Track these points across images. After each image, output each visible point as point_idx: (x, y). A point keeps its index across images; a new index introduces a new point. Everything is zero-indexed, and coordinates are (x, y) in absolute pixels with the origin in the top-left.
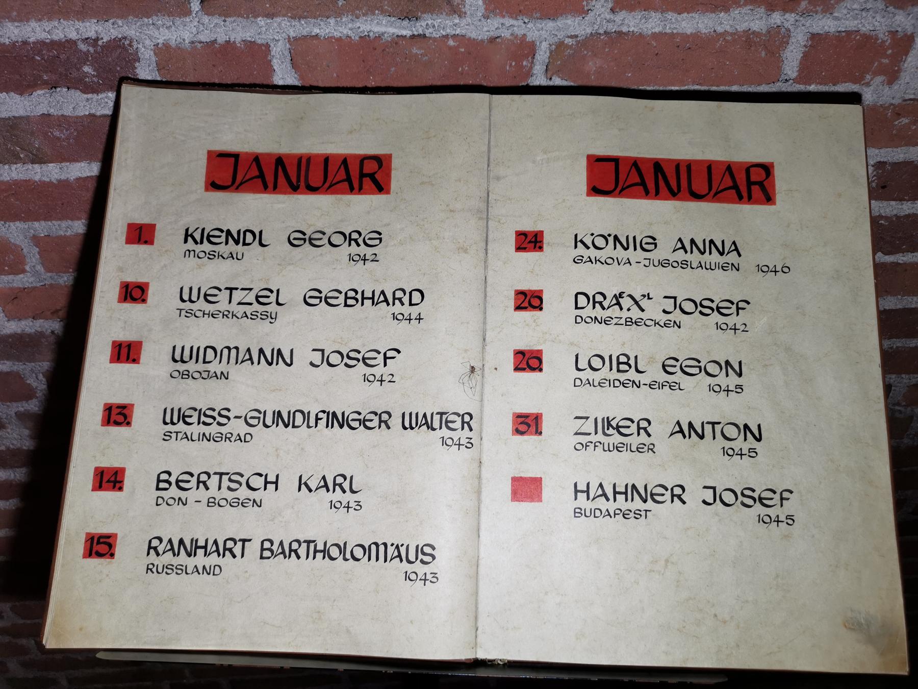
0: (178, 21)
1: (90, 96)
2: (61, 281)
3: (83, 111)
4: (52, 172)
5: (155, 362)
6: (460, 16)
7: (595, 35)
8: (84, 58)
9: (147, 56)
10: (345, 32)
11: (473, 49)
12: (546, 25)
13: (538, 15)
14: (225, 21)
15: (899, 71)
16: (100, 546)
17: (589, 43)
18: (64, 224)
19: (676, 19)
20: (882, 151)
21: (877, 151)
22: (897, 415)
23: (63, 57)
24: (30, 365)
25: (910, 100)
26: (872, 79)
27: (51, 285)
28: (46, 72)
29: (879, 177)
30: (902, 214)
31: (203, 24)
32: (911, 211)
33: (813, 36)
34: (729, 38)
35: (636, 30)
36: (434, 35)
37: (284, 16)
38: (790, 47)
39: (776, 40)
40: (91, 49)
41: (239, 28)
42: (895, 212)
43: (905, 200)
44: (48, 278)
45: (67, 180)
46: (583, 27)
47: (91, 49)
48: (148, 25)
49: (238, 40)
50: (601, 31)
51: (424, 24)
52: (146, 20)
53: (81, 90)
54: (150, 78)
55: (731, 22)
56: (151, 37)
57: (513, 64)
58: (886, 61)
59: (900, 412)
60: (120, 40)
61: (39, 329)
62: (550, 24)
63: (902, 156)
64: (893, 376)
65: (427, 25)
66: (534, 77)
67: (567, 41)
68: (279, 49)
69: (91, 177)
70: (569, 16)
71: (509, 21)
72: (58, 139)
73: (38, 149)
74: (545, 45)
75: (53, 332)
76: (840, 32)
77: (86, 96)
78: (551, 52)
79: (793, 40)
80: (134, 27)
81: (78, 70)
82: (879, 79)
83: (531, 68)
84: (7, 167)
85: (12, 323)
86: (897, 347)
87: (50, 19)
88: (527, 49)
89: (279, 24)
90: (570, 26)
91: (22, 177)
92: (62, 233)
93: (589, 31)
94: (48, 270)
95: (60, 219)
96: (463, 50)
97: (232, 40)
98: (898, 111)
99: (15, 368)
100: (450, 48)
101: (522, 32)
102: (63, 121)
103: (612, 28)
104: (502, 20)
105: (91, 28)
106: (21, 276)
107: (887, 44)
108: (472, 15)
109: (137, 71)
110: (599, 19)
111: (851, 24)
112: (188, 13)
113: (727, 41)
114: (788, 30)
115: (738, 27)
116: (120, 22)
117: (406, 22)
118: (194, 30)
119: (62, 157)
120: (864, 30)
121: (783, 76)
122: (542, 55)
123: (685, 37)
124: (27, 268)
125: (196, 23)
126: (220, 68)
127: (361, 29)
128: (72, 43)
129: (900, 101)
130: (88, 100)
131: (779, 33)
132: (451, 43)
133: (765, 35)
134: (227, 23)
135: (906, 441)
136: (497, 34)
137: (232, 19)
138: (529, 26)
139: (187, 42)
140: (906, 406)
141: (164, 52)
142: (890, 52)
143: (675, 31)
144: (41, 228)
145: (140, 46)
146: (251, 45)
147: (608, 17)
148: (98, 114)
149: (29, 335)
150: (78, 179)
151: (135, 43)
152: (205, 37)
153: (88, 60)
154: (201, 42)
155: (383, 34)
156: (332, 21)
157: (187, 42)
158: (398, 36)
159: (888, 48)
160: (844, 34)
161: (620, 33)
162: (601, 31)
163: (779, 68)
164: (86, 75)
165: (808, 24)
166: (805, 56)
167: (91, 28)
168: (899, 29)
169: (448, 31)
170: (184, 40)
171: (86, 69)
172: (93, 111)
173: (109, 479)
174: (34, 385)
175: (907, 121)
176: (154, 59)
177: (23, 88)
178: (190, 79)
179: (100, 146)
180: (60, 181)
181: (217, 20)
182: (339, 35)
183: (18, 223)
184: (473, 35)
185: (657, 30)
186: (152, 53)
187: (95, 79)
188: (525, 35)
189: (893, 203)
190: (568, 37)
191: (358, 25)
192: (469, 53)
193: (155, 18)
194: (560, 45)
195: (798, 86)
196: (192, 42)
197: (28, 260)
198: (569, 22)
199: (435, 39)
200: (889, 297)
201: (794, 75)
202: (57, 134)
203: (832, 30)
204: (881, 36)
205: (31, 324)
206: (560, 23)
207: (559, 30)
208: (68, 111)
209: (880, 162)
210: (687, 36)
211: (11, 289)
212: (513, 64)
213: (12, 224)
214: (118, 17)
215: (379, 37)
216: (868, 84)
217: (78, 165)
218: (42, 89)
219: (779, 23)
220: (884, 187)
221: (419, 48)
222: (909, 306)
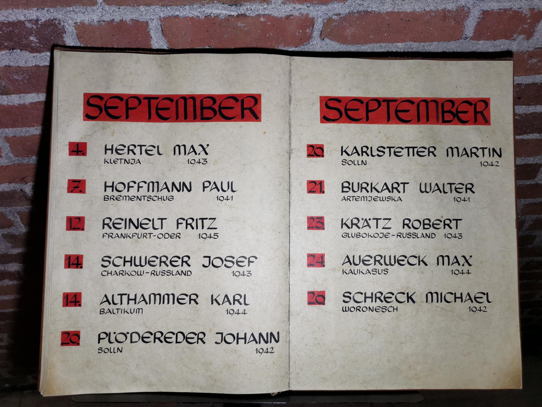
0: (89, 9)
1: (35, 54)
2: (25, 162)
3: (31, 64)
4: (15, 100)
5: (93, 226)
6: (268, 4)
7: (351, 14)
8: (30, 32)
9: (70, 30)
10: (196, 14)
11: (277, 24)
12: (321, 8)
13: (316, 2)
14: (119, 8)
15: (534, 31)
16: (71, 338)
17: (348, 18)
18: (24, 129)
19: (401, 4)
20: (519, 78)
24: (9, 209)
25: (539, 48)
26: (517, 37)
27: (18, 164)
28: (6, 41)
30: (529, 113)
31: (106, 11)
32: (534, 111)
34: (433, 14)
35: (376, 10)
36: (252, 15)
37: (157, 5)
38: (470, 19)
39: (462, 14)
40: (35, 27)
41: (128, 13)
42: (524, 112)
44: (16, 160)
45: (24, 104)
46: (344, 9)
48: (70, 11)
49: (128, 20)
50: (355, 11)
51: (245, 8)
52: (68, 8)
53: (29, 51)
54: (72, 44)
55: (434, 5)
56: (72, 19)
57: (301, 31)
60: (52, 20)
61: (13, 189)
62: (324, 7)
63: (531, 80)
65: (247, 9)
66: (313, 39)
68: (154, 25)
69: (39, 102)
70: (336, 3)
71: (298, 6)
72: (17, 80)
73: (4, 87)
74: (320, 20)
75: (21, 190)
77: (32, 54)
78: (324, 24)
79: (472, 14)
80: (61, 13)
81: (27, 39)
82: (522, 37)
83: (312, 33)
86: (520, 185)
87: (7, 9)
88: (309, 22)
89: (154, 10)
90: (336, 8)
92: (23, 135)
93: (347, 11)
94: (16, 156)
95: (22, 127)
96: (269, 24)
97: (124, 19)
98: (531, 55)
100: (261, 22)
101: (306, 12)
102: (19, 70)
103: (361, 9)
104: (294, 5)
105: (33, 14)
108: (275, 3)
109: (65, 39)
110: (354, 4)
111: (507, 5)
112: (95, 3)
114: (469, 8)
115: (439, 8)
116: (52, 10)
117: (233, 8)
118: (100, 14)
119: (18, 92)
120: (514, 8)
121: (464, 36)
123: (406, 14)
124: (3, 155)
125: (101, 10)
127: (206, 12)
128: (21, 23)
129: (532, 49)
130: (34, 57)
131: (463, 10)
132: (262, 19)
133: (455, 12)
134: (121, 10)
136: (291, 13)
137: (124, 7)
138: (310, 8)
139: (95, 21)
140: (522, 215)
141: (82, 29)
142: (529, 21)
143: (400, 11)
144: (10, 132)
145: (66, 24)
146: (136, 22)
147: (360, 2)
148: (41, 65)
149: (7, 192)
150: (31, 104)
151: (62, 22)
152: (107, 18)
154: (104, 21)
155: (220, 14)
156: (187, 7)
157: (95, 21)
158: (229, 16)
159: (529, 19)
160: (502, 11)
161: (367, 12)
162: (355, 11)
163: (462, 31)
164: (32, 42)
165: (481, 5)
166: (479, 24)
167: (33, 14)
168: (536, 7)
169: (260, 12)
170: (94, 20)
171: (32, 38)
172: (38, 64)
173: (72, 300)
174: (12, 219)
175: (536, 60)
176: (75, 32)
178: (98, 44)
179: (44, 84)
180: (19, 105)
181: (114, 8)
182: (192, 15)
184: (276, 15)
185: (389, 10)
186: (74, 28)
187: (38, 45)
188: (308, 14)
189: (524, 107)
190: (335, 15)
191: (204, 9)
192: (274, 26)
193: (74, 7)
194: (330, 20)
195: (473, 41)
196: (99, 22)
197: (3, 150)
198: (335, 6)
199: (252, 17)
201: (472, 35)
202: (16, 77)
203: (496, 8)
204: (524, 11)
205: (8, 186)
206: (330, 6)
207: (329, 11)
208: (22, 64)
209: (518, 84)
210: (408, 13)
212: (301, 31)
214: (50, 7)
215: (217, 16)
216: (515, 40)
217: (30, 95)
218: (4, 50)
219: (464, 4)
220: (519, 98)
221: (242, 23)
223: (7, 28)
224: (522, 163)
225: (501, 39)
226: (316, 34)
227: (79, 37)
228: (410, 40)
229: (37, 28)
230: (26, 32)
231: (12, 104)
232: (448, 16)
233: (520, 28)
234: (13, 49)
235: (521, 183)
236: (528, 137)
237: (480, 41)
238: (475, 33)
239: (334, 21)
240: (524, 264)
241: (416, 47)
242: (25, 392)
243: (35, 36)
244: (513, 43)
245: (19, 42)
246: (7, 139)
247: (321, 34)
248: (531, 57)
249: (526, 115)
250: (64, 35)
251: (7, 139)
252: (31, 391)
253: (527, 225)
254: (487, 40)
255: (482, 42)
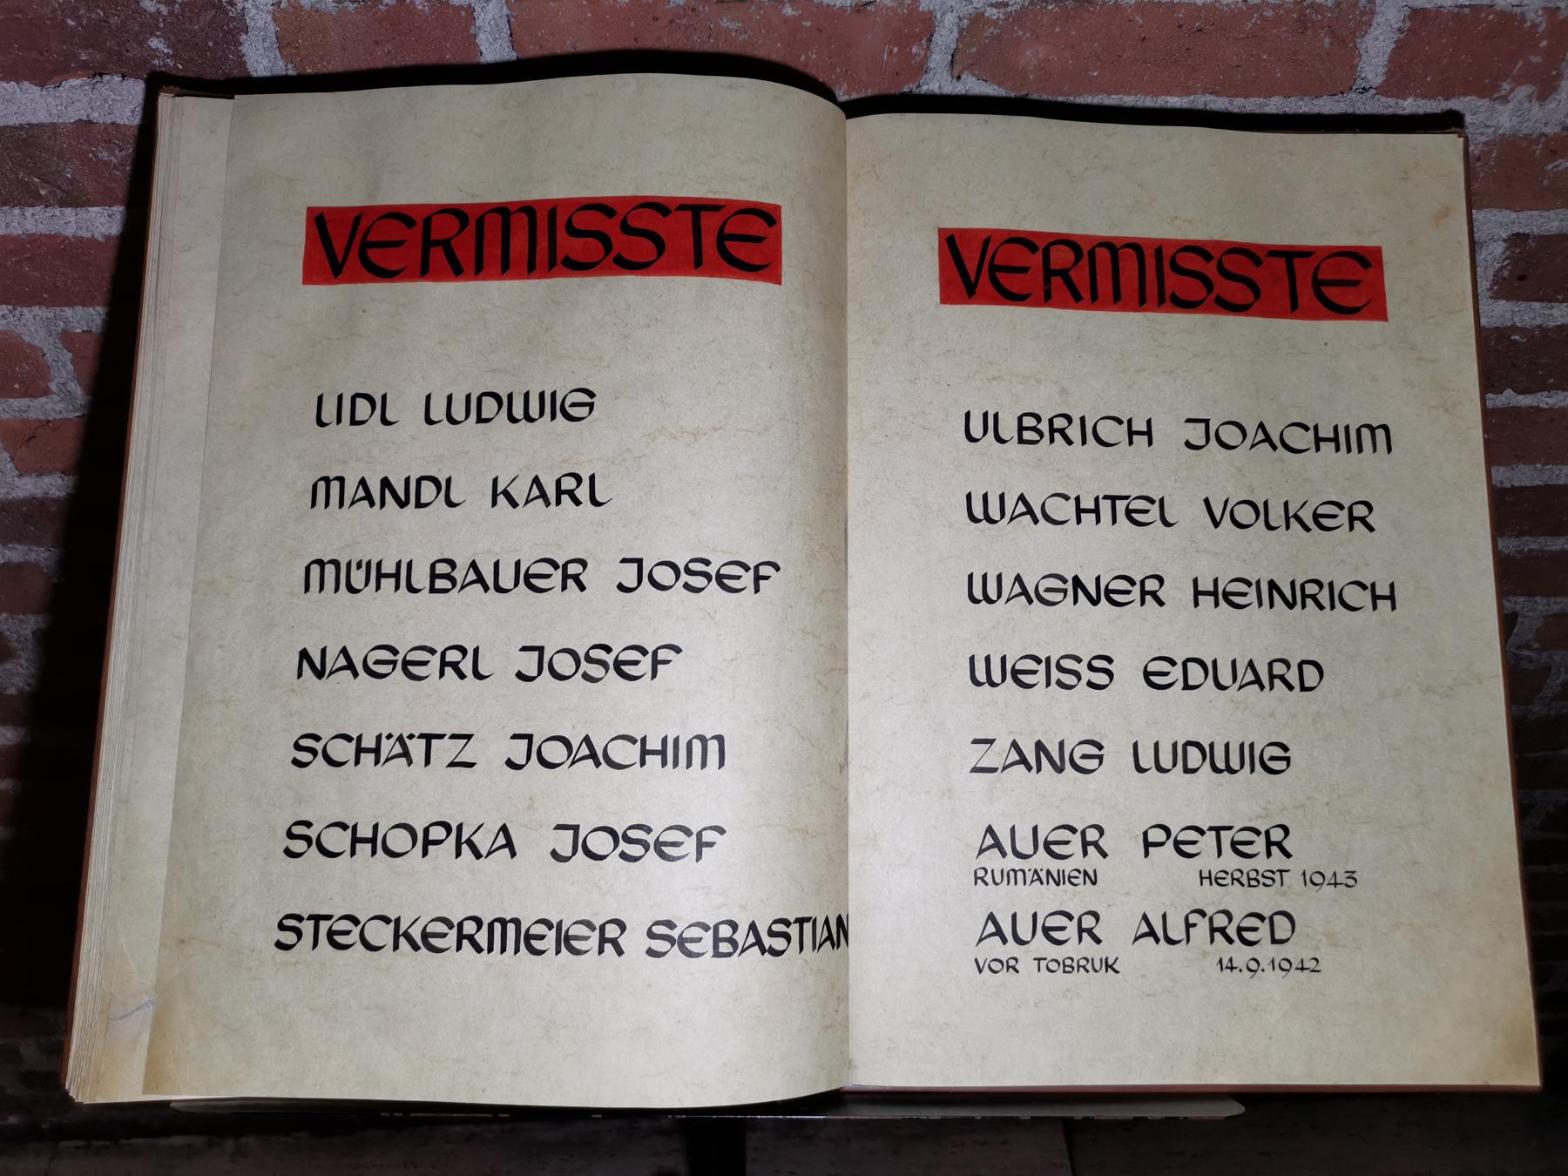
9: (260, 23)
15: (1559, 76)
20: (1523, 215)
21: (1514, 215)
22: (1524, 665)
23: (114, 20)
26: (1512, 90)
29: (1515, 261)
30: (1551, 324)
33: (1416, 14)
34: (1269, 13)
38: (1375, 32)
40: (164, 9)
42: (1538, 322)
43: (1556, 300)
47: (164, 9)
57: (895, 50)
58: (1536, 59)
59: (1530, 660)
63: (1556, 224)
64: (1522, 599)
67: (992, 13)
72: (106, 164)
73: (71, 182)
74: (950, 19)
76: (1461, 6)
78: (961, 32)
79: (1378, 19)
81: (141, 43)
82: (1524, 91)
83: (926, 58)
84: (17, 211)
85: (26, 480)
86: (1531, 551)
91: (42, 229)
96: (808, 24)
99: (32, 557)
100: (787, 20)
106: (43, 400)
107: (1541, 29)
109: (244, 49)
113: (1265, 19)
121: (1359, 81)
122: (946, 35)
124: (53, 386)
126: (389, 47)
129: (1557, 129)
135: (1536, 708)
142: (1544, 43)
145: (248, 5)
153: (158, 29)
160: (1467, 11)
163: (1353, 67)
166: (1399, 48)
171: (155, 43)
176: (272, 28)
177: (45, 74)
183: (36, 309)
186: (269, 18)
187: (170, 62)
189: (1536, 305)
190: (991, 5)
192: (820, 31)
194: (978, 19)
195: (1383, 99)
197: (54, 373)
200: (1521, 466)
201: (1379, 80)
202: (104, 155)
204: (1530, 15)
210: (1198, 8)
211: (25, 422)
212: (895, 50)
213: (25, 310)
216: (1505, 99)
218: (78, 77)
220: (1522, 278)
222: (1554, 482)
223: (89, 10)
224: (1536, 483)
225: (1465, 95)
226: (938, 59)
227: (284, 44)
228: (1205, 91)
229: (171, 13)
230: (141, 26)
231: (88, 235)
232: (1313, 22)
233: (1520, 63)
234: (101, 75)
235: (1534, 546)
236: (1551, 401)
237: (1405, 99)
238: (1390, 74)
239: (990, 22)
240: (1551, 809)
241: (1218, 103)
242: (64, 1144)
243: (165, 37)
244: (1499, 108)
245: (121, 54)
246: (67, 339)
247: (952, 63)
248: (1553, 154)
249: (1544, 330)
250: (243, 37)
251: (67, 339)
252: (81, 1143)
253: (1555, 682)
254: (1424, 97)
255: (1410, 100)
